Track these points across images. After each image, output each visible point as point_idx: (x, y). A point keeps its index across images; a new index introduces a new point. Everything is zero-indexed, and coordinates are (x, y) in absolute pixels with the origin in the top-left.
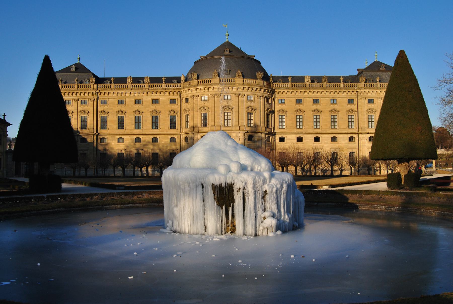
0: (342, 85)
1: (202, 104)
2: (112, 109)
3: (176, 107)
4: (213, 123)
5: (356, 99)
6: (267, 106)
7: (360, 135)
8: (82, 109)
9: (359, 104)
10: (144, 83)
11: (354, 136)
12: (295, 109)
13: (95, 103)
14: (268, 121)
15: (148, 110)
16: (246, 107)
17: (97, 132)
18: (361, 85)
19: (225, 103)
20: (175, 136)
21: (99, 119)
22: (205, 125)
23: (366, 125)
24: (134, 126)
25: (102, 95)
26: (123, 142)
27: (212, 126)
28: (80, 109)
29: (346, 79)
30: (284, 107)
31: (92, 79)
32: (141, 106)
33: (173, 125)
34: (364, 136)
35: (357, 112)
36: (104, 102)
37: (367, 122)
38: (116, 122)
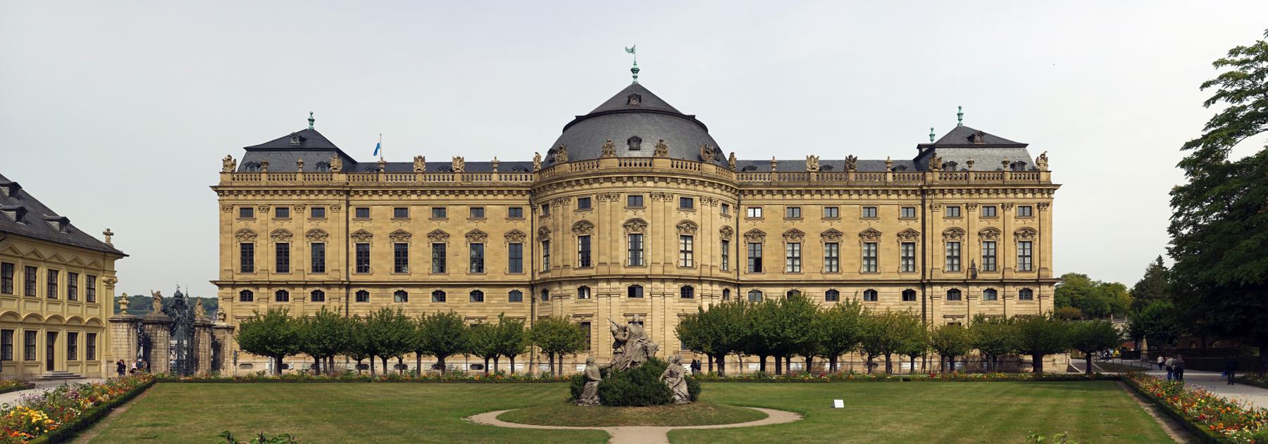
0: (890, 177)
1: (580, 217)
3: (523, 226)
4: (603, 259)
5: (919, 209)
7: (928, 290)
10: (452, 171)
11: (914, 288)
14: (725, 257)
15: (460, 232)
16: (677, 222)
18: (933, 177)
19: (630, 214)
20: (521, 290)
21: (353, 250)
23: (941, 266)
24: (430, 265)
25: (357, 197)
27: (600, 264)
28: (308, 226)
29: (899, 167)
30: (759, 226)
31: (336, 162)
32: (443, 223)
33: (515, 263)
34: (937, 289)
35: (920, 237)
36: (363, 212)
37: (941, 259)
38: (392, 257)
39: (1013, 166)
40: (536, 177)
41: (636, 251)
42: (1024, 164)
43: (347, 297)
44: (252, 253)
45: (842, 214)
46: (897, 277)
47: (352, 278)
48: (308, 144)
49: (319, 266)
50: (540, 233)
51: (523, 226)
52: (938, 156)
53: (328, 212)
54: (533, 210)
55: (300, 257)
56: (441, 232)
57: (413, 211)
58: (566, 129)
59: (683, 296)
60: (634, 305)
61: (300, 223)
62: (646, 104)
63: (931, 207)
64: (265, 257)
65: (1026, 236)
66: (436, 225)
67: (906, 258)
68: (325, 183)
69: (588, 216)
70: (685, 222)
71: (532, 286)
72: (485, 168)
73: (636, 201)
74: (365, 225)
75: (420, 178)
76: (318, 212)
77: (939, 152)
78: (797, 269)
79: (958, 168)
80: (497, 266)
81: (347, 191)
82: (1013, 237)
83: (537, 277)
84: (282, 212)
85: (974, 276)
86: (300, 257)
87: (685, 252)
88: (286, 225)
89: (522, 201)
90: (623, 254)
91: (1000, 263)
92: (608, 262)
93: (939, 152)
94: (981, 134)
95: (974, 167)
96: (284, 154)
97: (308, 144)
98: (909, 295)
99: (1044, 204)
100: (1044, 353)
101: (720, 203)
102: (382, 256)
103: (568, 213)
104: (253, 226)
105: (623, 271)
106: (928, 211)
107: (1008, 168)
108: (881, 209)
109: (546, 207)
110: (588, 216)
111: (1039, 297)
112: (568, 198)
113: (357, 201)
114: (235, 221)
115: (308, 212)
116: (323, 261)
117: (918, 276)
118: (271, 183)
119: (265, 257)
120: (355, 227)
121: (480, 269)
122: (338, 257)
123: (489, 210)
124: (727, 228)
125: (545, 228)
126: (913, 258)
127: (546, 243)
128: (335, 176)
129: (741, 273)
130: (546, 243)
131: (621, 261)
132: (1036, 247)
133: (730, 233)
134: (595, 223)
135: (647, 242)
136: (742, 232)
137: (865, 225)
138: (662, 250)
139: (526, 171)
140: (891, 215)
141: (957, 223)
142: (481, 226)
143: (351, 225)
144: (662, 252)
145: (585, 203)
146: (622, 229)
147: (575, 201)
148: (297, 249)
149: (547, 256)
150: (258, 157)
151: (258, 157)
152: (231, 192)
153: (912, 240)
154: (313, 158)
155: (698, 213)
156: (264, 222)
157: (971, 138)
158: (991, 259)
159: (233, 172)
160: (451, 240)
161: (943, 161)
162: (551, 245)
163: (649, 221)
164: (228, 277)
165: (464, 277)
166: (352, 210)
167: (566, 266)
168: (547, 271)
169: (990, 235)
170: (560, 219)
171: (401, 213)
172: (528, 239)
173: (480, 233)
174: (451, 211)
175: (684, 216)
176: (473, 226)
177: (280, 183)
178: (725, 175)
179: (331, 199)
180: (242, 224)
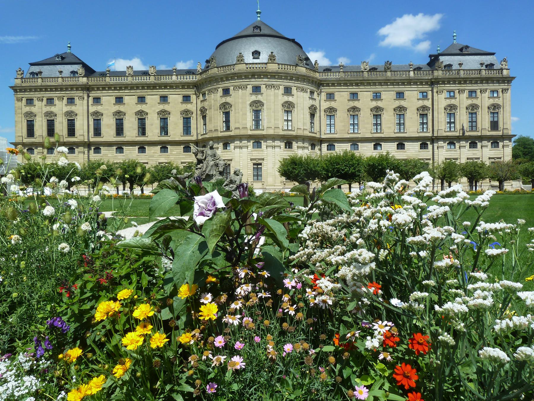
0: (412, 74)
1: (224, 100)
2: (108, 109)
3: (191, 107)
4: (237, 125)
5: (430, 93)
6: (311, 102)
8: (68, 110)
9: (434, 98)
12: (348, 107)
13: (85, 102)
15: (154, 111)
17: (88, 139)
19: (254, 98)
21: (91, 123)
22: (228, 128)
23: (443, 128)
24: (136, 131)
26: (123, 153)
28: (66, 109)
30: (333, 104)
32: (144, 106)
33: (187, 129)
39: (486, 66)
40: (198, 77)
41: (257, 121)
42: (492, 65)
43: (89, 152)
44: (33, 125)
45: (383, 97)
46: (417, 135)
47: (92, 140)
48: (66, 61)
49: (71, 132)
50: (201, 110)
51: (191, 107)
52: (441, 61)
53: (77, 101)
54: (198, 97)
55: (61, 127)
56: (143, 111)
57: (126, 99)
58: (216, 49)
59: (286, 148)
60: (257, 154)
61: (60, 108)
62: (265, 31)
63: (437, 92)
64: (40, 128)
65: (495, 109)
66: (140, 107)
67: (423, 124)
68: (74, 83)
69: (228, 99)
70: (286, 102)
71: (196, 143)
72: (169, 73)
73: (257, 89)
74: (99, 108)
75: (130, 79)
76: (71, 101)
77: (442, 58)
78: (356, 131)
79: (454, 68)
80: (176, 131)
81: (87, 88)
82: (487, 110)
83: (200, 137)
84: (50, 101)
85: (464, 133)
86: (61, 127)
87: (287, 121)
88: (53, 109)
89: (190, 92)
90: (249, 122)
91: (479, 125)
92: (241, 127)
93: (442, 58)
94: (467, 47)
95: (463, 67)
96: (52, 67)
97: (66, 61)
98: (424, 146)
99: (505, 89)
100: (506, 180)
101: (309, 91)
102: (108, 126)
103: (216, 98)
104: (34, 109)
105: (250, 133)
106: (435, 94)
107: (484, 67)
108: (406, 94)
109: (204, 95)
110: (228, 99)
111: (503, 146)
112: (216, 89)
113: (94, 94)
114: (23, 107)
115: (65, 101)
116: (74, 130)
117: (430, 135)
118: (43, 84)
119: (40, 128)
120: (92, 109)
121: (166, 133)
122: (83, 130)
123: (171, 98)
124: (313, 106)
125: (204, 107)
126: (427, 123)
127: (204, 117)
128: (80, 79)
129: (322, 133)
130: (204, 117)
131: (248, 127)
132: (501, 116)
133: (315, 109)
134: (232, 103)
135: (264, 115)
136: (323, 108)
137: (397, 103)
138: (273, 121)
139: (193, 74)
140: (413, 97)
141: (453, 101)
142: (166, 107)
143: (90, 108)
144: (273, 120)
145: (226, 92)
146: (248, 107)
147: (220, 90)
148: (59, 123)
149: (205, 124)
150: (36, 69)
151: (36, 69)
152: (21, 91)
153: (426, 112)
154: (67, 69)
155: (295, 97)
156: (40, 108)
157: (461, 50)
158: (473, 124)
159: (22, 78)
160: (149, 116)
161: (444, 64)
162: (207, 118)
163: (264, 102)
164: (19, 140)
165: (157, 138)
166: (91, 99)
167: (216, 130)
168: (206, 134)
169: (473, 110)
170: (213, 102)
171: (119, 100)
172: (194, 115)
173: (165, 111)
174: (148, 99)
175: (286, 98)
176: (161, 107)
177: (49, 84)
178: (312, 74)
179: (80, 93)
180: (27, 109)
